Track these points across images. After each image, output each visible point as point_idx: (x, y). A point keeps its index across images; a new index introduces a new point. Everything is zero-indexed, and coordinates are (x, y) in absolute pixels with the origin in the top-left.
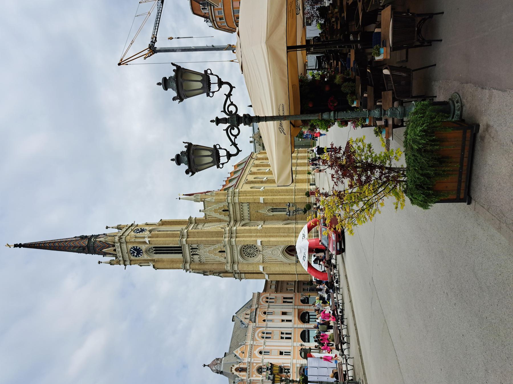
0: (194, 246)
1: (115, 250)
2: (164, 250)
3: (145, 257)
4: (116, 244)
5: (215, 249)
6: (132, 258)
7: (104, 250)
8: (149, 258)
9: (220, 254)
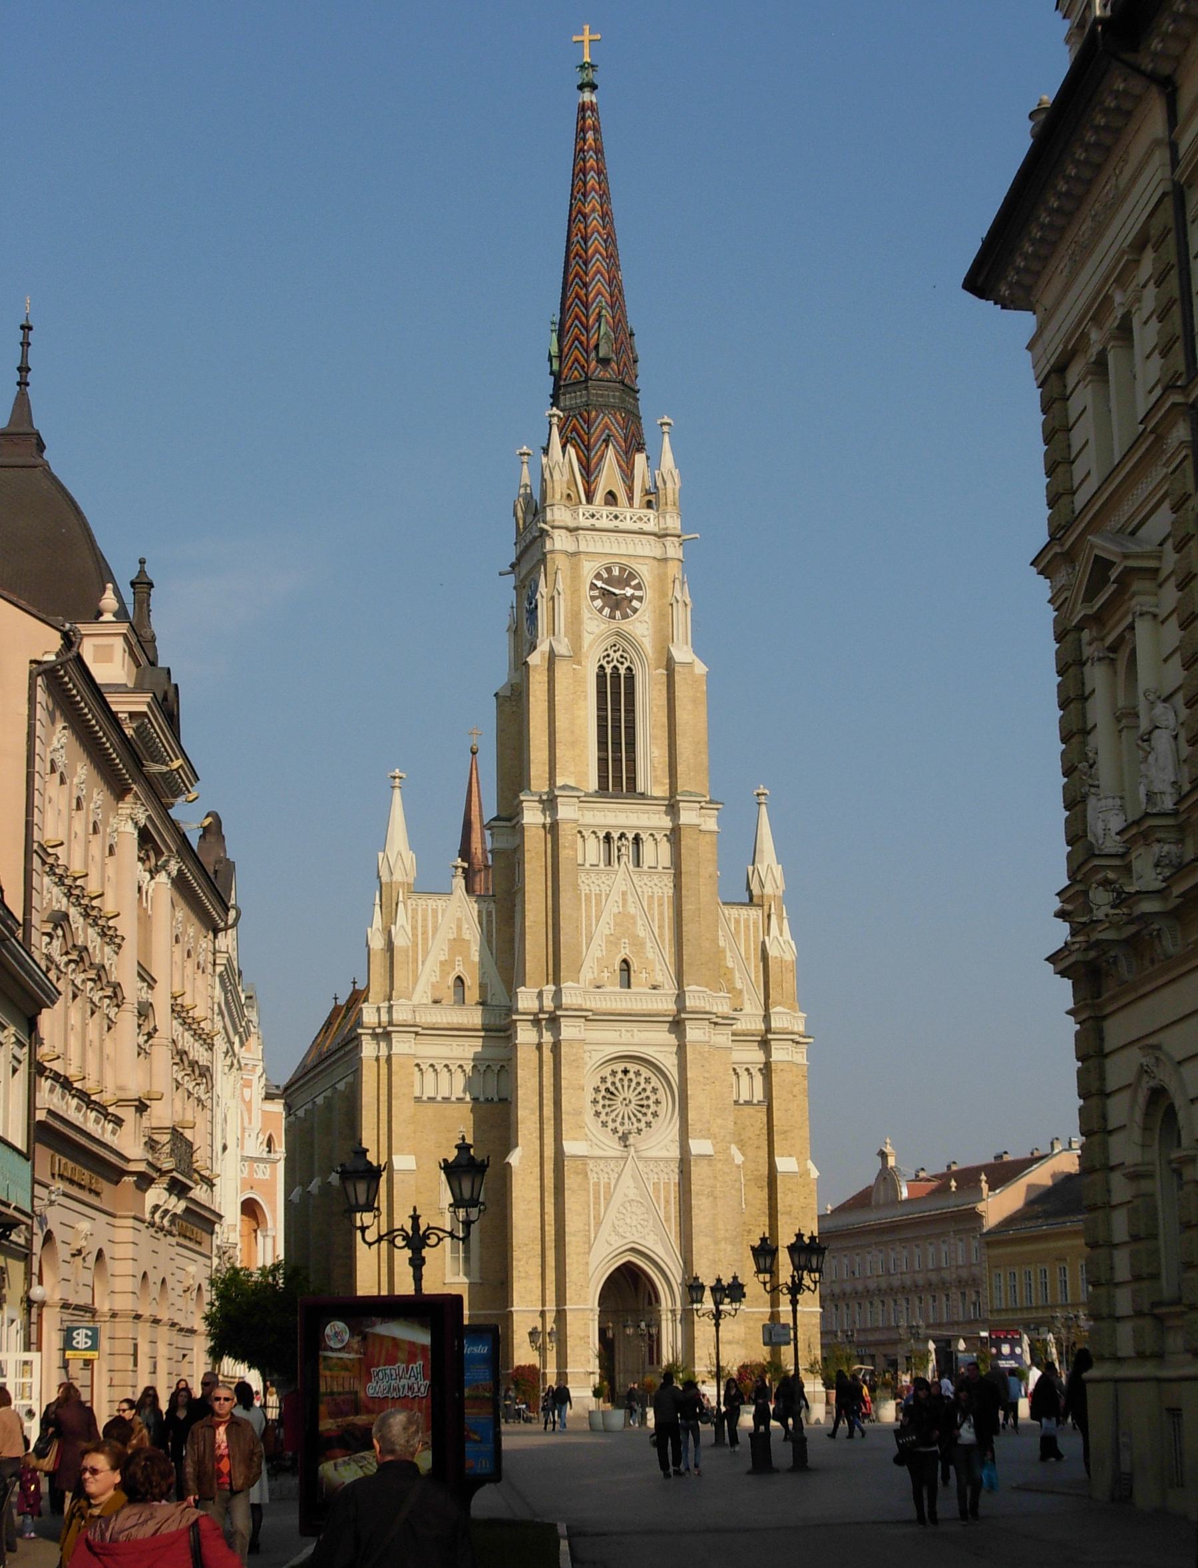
3: (596, 628)
4: (651, 513)
5: (637, 944)
8: (587, 640)
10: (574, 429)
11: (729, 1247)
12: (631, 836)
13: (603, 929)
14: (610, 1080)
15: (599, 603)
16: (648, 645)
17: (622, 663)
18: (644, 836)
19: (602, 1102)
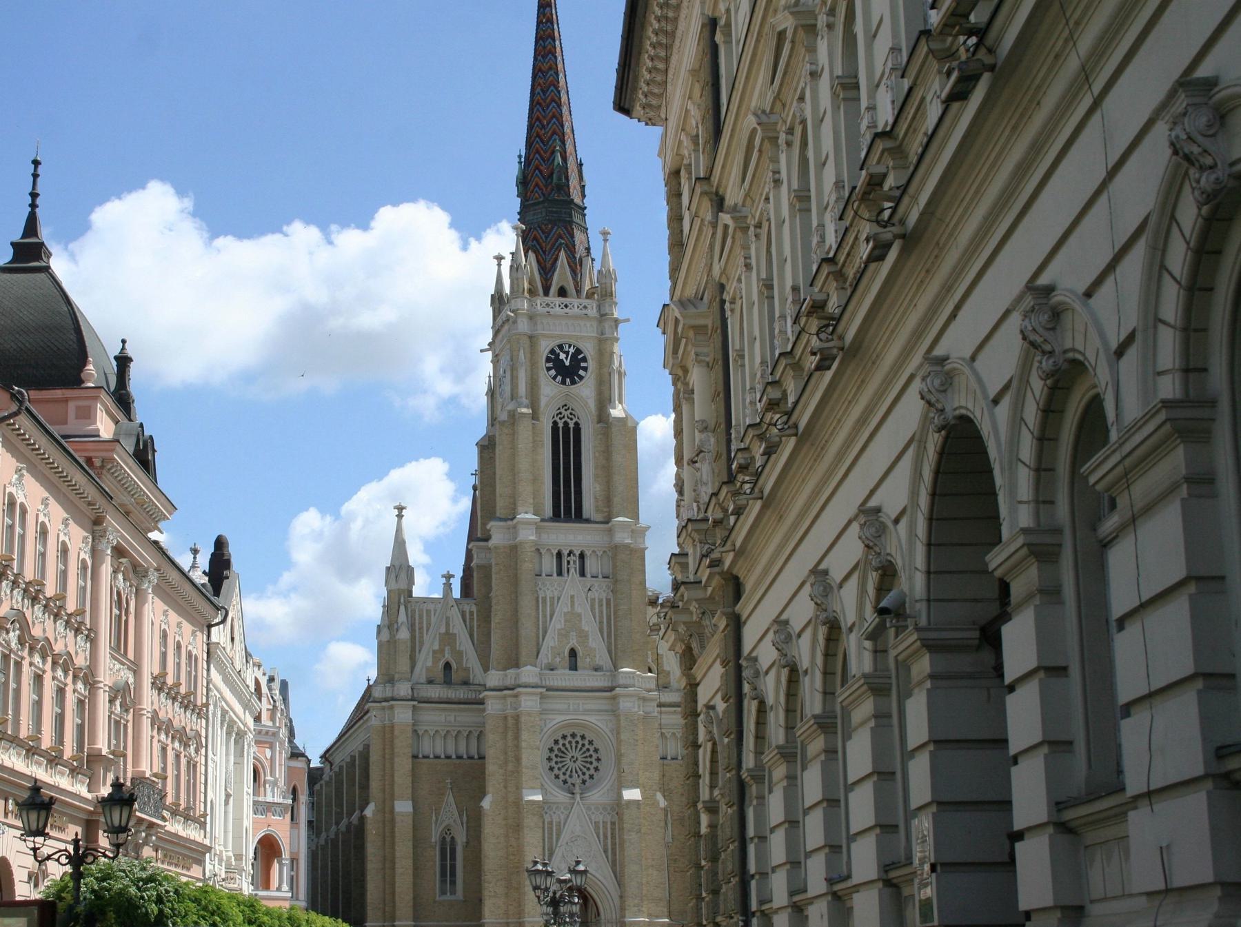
0: (591, 565)
1: (562, 292)
2: (567, 455)
3: (550, 389)
5: (583, 636)
6: (545, 347)
7: (562, 255)
8: (543, 401)
9: (567, 653)
10: (535, 238)
11: (655, 873)
12: (577, 553)
13: (557, 624)
14: (561, 742)
15: (553, 372)
16: (592, 404)
18: (588, 553)
19: (555, 759)
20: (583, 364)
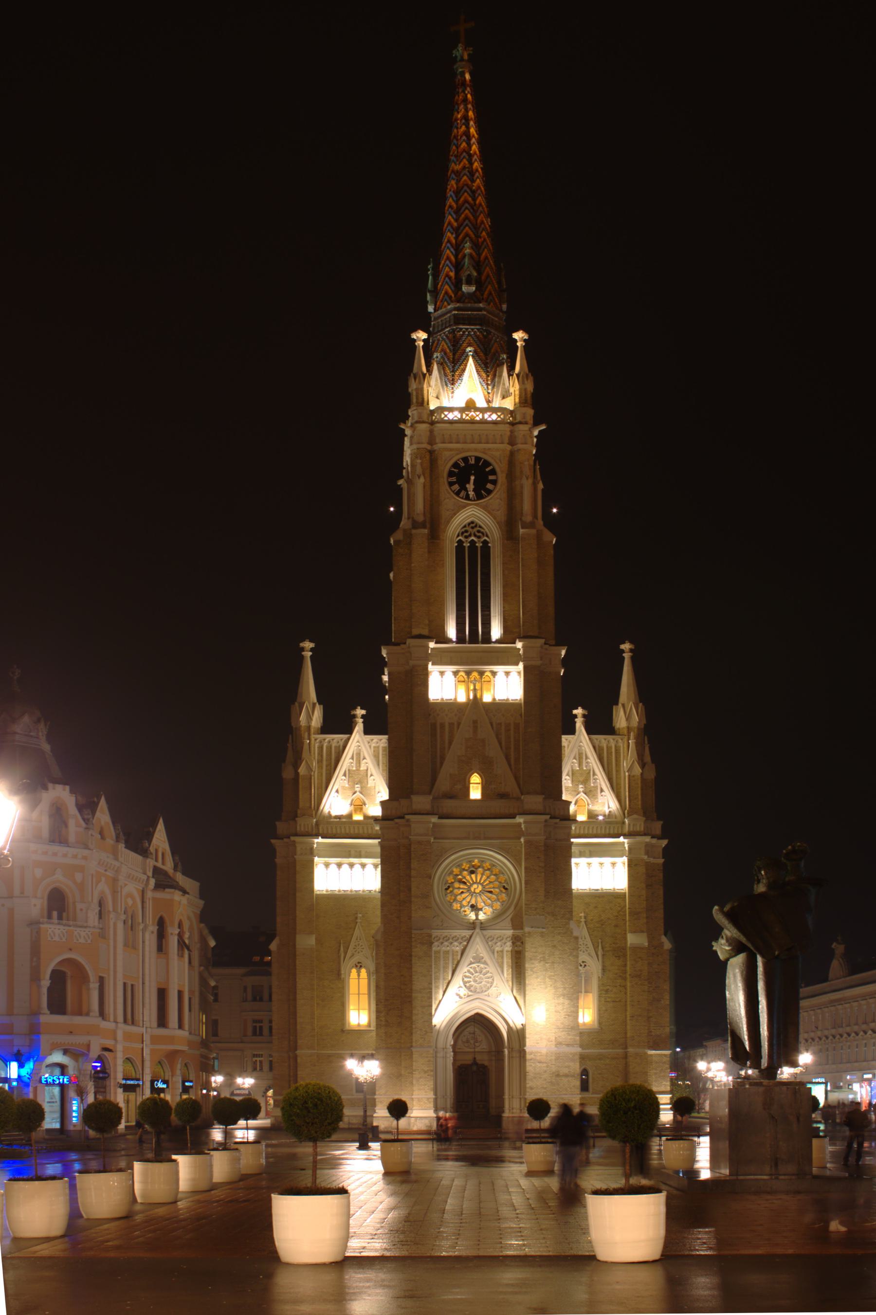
17: (479, 537)
20: (491, 477)
